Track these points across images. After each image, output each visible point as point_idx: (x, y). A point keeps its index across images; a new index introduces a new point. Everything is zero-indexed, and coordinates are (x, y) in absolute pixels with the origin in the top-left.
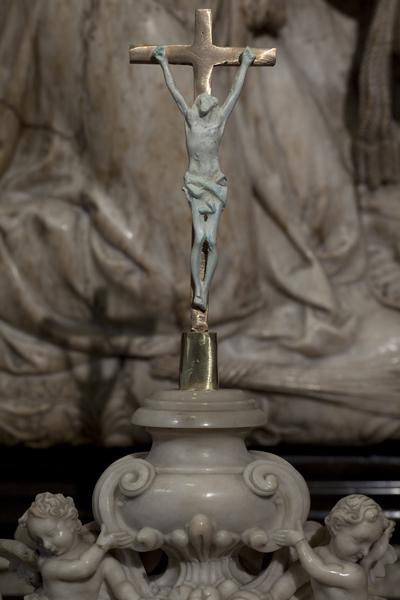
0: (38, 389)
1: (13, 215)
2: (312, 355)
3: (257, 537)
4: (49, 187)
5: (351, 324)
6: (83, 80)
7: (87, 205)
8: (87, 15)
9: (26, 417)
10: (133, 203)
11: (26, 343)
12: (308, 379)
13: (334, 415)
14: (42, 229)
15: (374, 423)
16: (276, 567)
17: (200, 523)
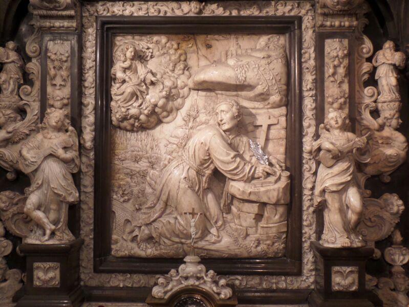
0: (168, 248)
1: (165, 220)
2: (214, 243)
3: (199, 275)
4: (171, 215)
5: (220, 238)
6: (177, 199)
7: (176, 218)
8: (177, 190)
9: (166, 253)
10: (184, 219)
11: (166, 241)
12: (213, 247)
13: (217, 253)
14: (170, 223)
15: (224, 255)
16: (201, 279)
17: (191, 273)
